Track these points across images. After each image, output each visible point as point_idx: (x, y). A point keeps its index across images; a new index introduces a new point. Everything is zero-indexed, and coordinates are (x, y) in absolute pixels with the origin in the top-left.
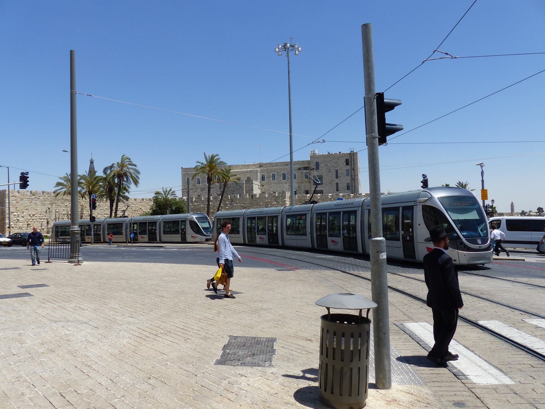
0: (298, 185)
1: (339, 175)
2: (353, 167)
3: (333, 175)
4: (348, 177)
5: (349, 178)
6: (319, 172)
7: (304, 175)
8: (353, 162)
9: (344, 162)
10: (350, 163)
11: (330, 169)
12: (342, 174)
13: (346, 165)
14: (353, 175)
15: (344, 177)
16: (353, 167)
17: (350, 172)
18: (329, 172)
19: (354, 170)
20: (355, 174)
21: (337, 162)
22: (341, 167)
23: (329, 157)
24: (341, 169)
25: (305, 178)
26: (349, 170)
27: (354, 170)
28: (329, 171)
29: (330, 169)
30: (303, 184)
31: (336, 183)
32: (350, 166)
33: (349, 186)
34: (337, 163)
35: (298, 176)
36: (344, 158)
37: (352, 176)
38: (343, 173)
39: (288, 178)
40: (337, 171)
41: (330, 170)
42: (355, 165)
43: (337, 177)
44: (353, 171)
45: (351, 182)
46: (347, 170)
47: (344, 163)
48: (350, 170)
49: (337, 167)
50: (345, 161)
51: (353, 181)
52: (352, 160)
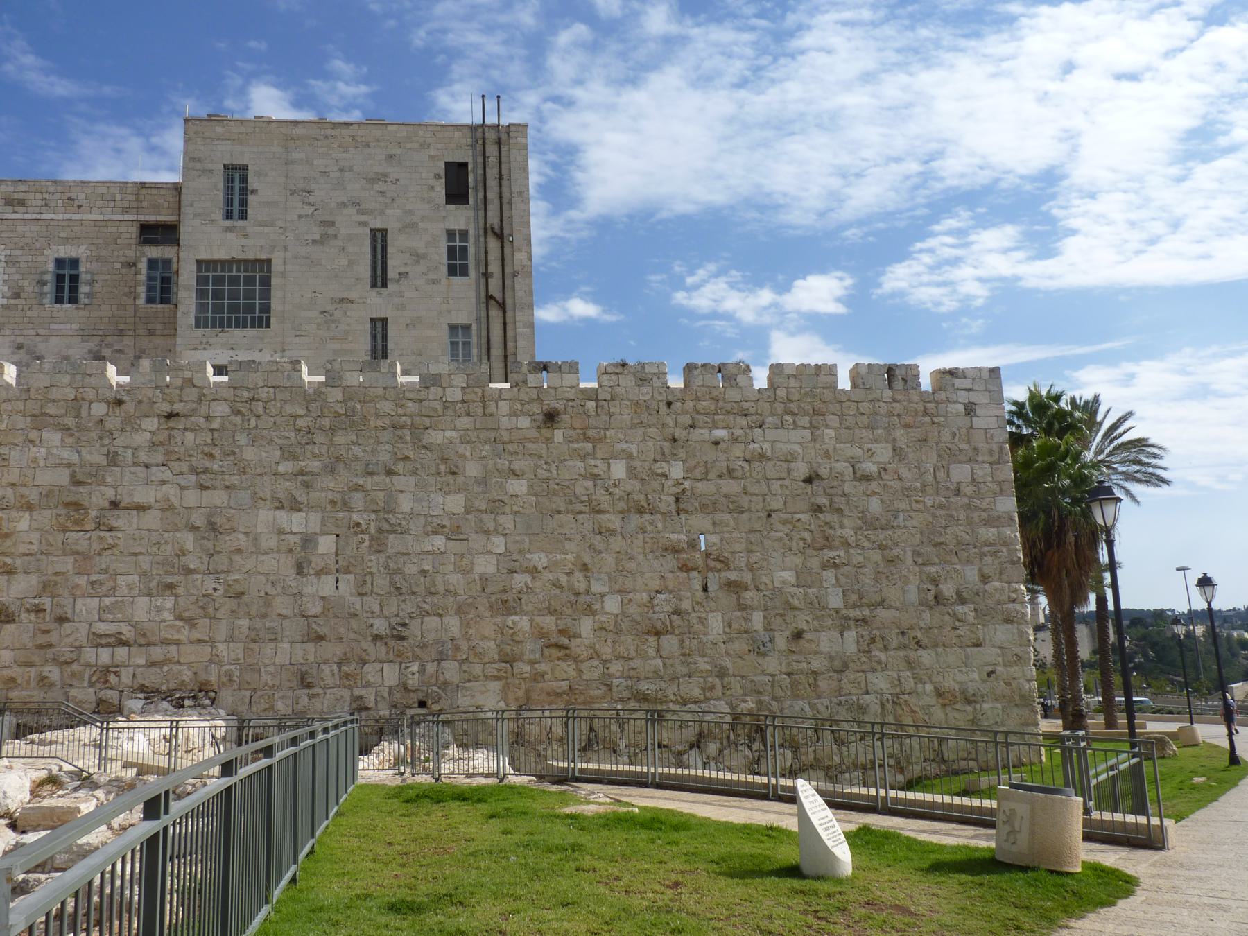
0: (92, 344)
1: (395, 265)
2: (493, 219)
3: (351, 263)
4: (458, 280)
5: (465, 289)
6: (246, 236)
7: (143, 277)
8: (492, 183)
9: (432, 182)
10: (475, 189)
11: (332, 224)
12: (418, 257)
13: (448, 201)
14: (494, 268)
15: (434, 282)
16: (493, 219)
17: (471, 251)
18: (324, 239)
19: (500, 236)
20: (508, 270)
21: (383, 177)
22: (411, 212)
23: (326, 137)
24: (409, 227)
25: (150, 300)
26: (464, 235)
27: (500, 236)
28: (322, 235)
29: (332, 224)
30: (128, 341)
31: (373, 321)
32: (476, 209)
33: (466, 344)
34: (380, 186)
35: (92, 283)
36: (431, 157)
37: (486, 275)
38: (421, 251)
39: (17, 295)
40: (379, 240)
41: (331, 231)
42: (510, 203)
43: (379, 279)
44: (493, 244)
45: (478, 320)
46: (451, 234)
47: (432, 187)
48: (472, 239)
49: (382, 212)
50: (437, 176)
51: (495, 313)
52: (492, 173)
